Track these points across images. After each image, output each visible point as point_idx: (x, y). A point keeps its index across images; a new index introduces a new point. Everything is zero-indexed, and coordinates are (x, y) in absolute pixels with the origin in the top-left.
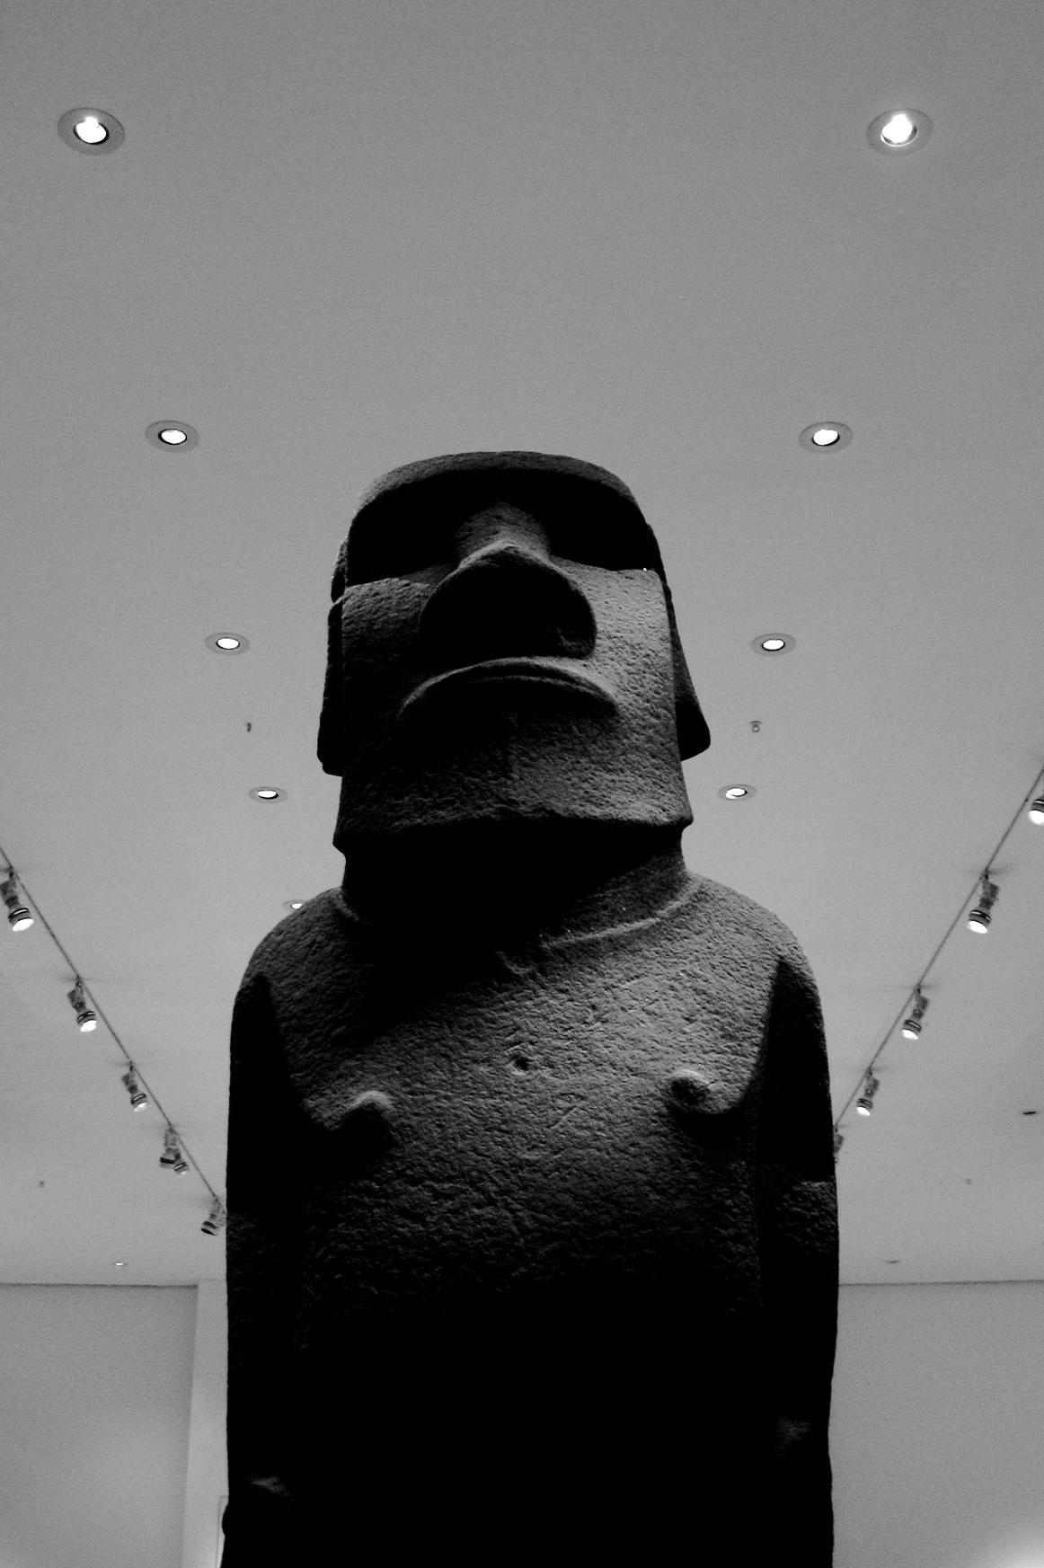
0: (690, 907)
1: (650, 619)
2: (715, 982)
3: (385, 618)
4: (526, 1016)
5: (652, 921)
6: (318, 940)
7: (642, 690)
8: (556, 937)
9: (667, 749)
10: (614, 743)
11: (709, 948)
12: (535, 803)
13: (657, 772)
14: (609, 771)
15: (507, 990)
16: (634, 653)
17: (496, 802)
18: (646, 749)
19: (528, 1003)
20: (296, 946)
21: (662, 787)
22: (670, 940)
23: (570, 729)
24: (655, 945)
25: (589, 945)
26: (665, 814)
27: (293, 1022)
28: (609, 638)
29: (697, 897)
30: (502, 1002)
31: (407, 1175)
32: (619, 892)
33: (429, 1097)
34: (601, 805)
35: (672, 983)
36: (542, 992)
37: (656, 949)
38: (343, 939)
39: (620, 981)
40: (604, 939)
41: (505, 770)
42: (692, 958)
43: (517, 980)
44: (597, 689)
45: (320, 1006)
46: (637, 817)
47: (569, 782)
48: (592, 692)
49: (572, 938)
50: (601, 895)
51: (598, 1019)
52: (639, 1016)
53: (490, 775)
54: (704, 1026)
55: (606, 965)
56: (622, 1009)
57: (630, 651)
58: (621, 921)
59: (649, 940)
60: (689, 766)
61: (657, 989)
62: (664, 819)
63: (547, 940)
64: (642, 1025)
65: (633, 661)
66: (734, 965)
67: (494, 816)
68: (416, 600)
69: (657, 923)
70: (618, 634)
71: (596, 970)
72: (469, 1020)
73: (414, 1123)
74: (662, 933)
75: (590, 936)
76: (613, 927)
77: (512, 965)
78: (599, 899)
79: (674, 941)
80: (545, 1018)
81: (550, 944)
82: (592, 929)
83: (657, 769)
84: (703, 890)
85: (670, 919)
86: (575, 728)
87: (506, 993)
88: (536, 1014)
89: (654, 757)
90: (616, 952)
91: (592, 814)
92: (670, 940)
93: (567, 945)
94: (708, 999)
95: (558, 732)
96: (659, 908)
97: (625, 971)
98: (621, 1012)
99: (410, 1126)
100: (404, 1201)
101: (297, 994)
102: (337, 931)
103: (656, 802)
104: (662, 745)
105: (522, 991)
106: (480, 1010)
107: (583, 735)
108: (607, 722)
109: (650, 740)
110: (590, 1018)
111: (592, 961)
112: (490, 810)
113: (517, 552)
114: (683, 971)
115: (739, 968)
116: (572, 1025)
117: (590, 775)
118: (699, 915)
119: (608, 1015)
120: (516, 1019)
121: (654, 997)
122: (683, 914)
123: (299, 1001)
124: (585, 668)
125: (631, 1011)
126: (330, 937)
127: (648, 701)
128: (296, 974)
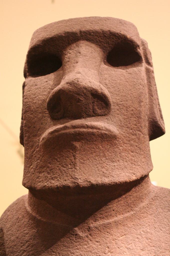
0: (149, 204)
1: (135, 94)
2: (154, 234)
3: (37, 98)
4: (85, 252)
5: (132, 213)
6: (20, 217)
7: (129, 125)
8: (96, 222)
9: (139, 148)
10: (116, 149)
11: (154, 220)
12: (84, 179)
13: (133, 158)
14: (113, 162)
15: (78, 242)
16: (127, 110)
17: (71, 178)
18: (129, 150)
19: (86, 247)
20: (13, 218)
21: (134, 164)
22: (139, 219)
23: (99, 147)
24: (133, 222)
25: (107, 224)
26: (134, 176)
28: (118, 105)
29: (153, 199)
30: (77, 246)
32: (119, 204)
34: (108, 177)
35: (138, 236)
36: (90, 242)
37: (133, 223)
38: (27, 219)
39: (118, 237)
40: (113, 222)
41: (74, 165)
42: (147, 225)
44: (109, 131)
45: (19, 244)
46: (122, 180)
47: (97, 169)
48: (107, 132)
49: (101, 222)
50: (112, 206)
51: (109, 251)
52: (124, 250)
53: (70, 167)
54: (148, 252)
55: (113, 231)
56: (118, 248)
57: (125, 109)
58: (120, 214)
59: (131, 220)
60: (154, 144)
61: (132, 239)
62: (134, 178)
63: (92, 223)
64: (125, 253)
65: (126, 114)
66: (164, 226)
67: (70, 184)
68: (49, 90)
69: (134, 214)
70: (121, 103)
71: (110, 233)
74: (136, 217)
75: (108, 221)
76: (117, 217)
77: (80, 233)
78: (110, 208)
79: (141, 219)
80: (91, 252)
81: (94, 225)
82: (109, 218)
83: (133, 157)
84: (156, 195)
85: (140, 211)
86: (101, 147)
87: (78, 243)
88: (88, 251)
89: (132, 152)
90: (117, 226)
91: (104, 181)
92: (139, 219)
93: (99, 225)
94: (151, 241)
95: (94, 148)
96: (135, 207)
97: (121, 233)
98: (117, 249)
101: (12, 238)
102: (25, 215)
103: (131, 171)
104: (136, 146)
105: (83, 242)
106: (69, 249)
107: (104, 149)
108: (113, 142)
109: (131, 145)
110: (107, 251)
111: (108, 230)
112: (68, 182)
113: (78, 81)
114: (143, 231)
115: (166, 227)
116: (100, 254)
117: (106, 165)
118: (153, 206)
119: (113, 250)
120: (81, 252)
121: (130, 242)
122: (145, 208)
124: (106, 120)
125: (121, 248)
126: (23, 217)
127: (132, 129)
128: (12, 230)
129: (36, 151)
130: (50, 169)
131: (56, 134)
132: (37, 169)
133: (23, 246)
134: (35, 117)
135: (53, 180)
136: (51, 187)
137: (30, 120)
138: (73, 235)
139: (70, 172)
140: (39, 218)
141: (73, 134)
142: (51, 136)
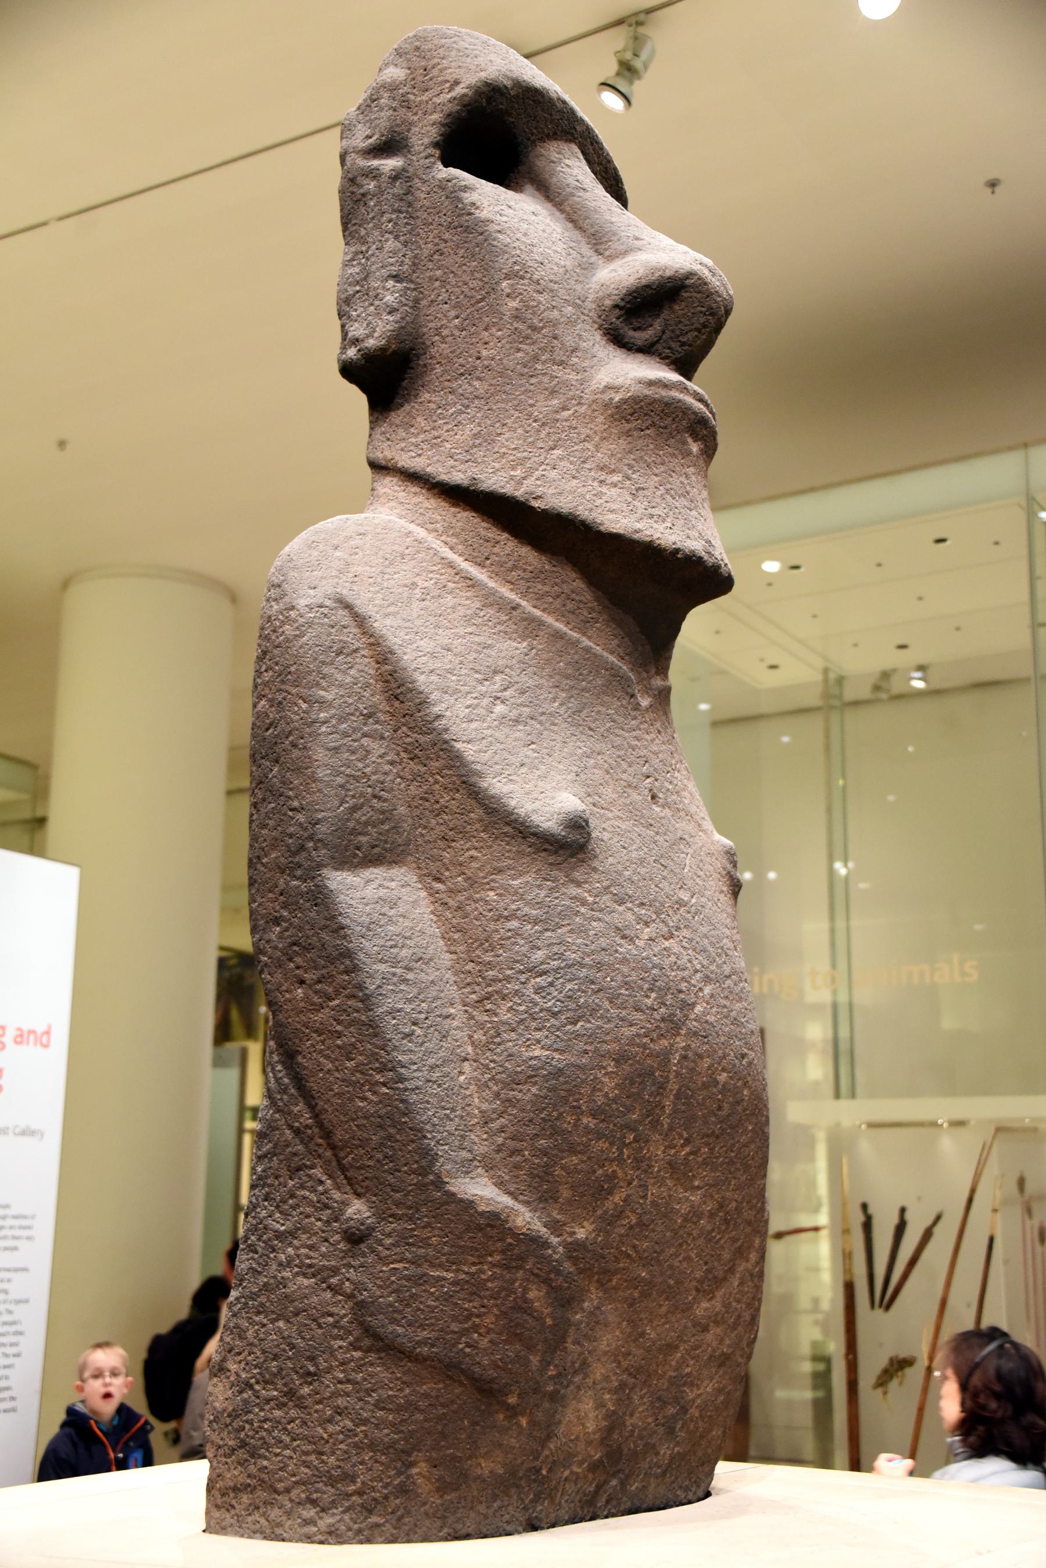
27: (434, 678)
31: (611, 893)
33: (610, 815)
43: (637, 707)
45: (463, 672)
72: (618, 741)
73: (605, 838)
99: (602, 840)
100: (616, 919)
101: (425, 644)
123: (433, 655)
129: (573, 414)
130: (638, 486)
131: (664, 393)
132: (590, 470)
133: (487, 683)
134: (554, 307)
135: (656, 522)
136: (658, 542)
137: (536, 307)
138: (627, 693)
139: (691, 519)
140: (537, 613)
141: (695, 413)
142: (647, 392)
